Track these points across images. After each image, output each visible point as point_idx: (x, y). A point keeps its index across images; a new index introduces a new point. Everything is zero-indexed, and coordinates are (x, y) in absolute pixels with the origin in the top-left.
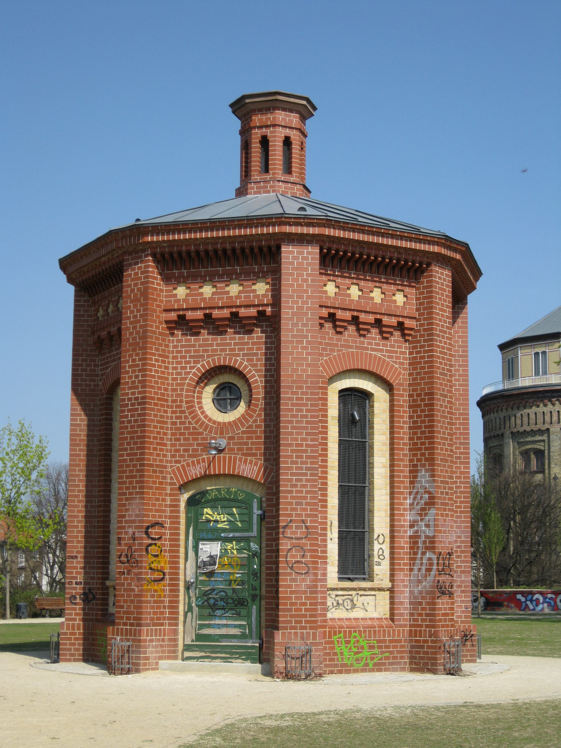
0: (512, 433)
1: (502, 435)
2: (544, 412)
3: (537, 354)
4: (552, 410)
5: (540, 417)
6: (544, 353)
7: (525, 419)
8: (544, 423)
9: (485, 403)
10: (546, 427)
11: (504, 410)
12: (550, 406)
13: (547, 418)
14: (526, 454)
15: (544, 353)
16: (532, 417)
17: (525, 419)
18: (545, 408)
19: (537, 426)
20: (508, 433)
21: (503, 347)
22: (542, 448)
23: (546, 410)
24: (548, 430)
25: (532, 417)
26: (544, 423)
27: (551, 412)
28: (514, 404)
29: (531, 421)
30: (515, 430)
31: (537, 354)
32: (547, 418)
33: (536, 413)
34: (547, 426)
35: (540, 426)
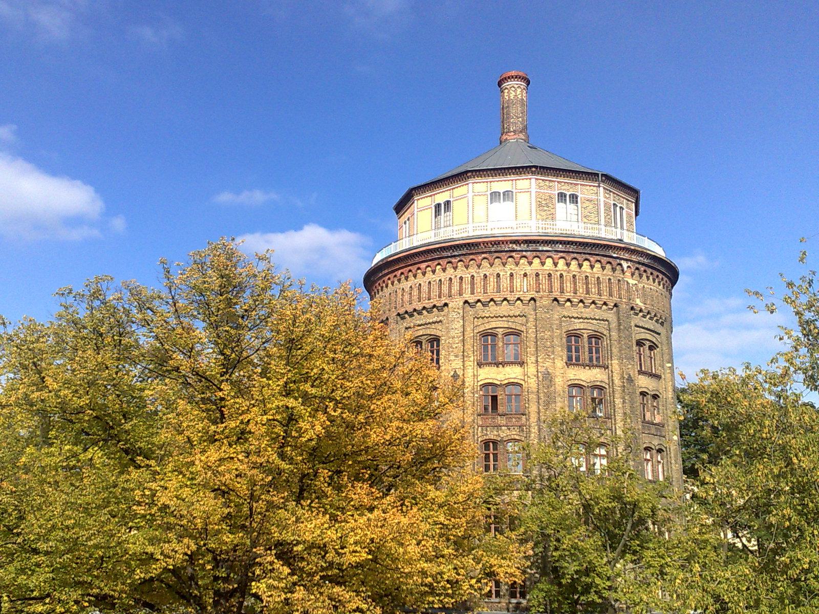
0: (399, 314)
1: (387, 319)
2: (440, 280)
4: (452, 277)
5: (435, 288)
6: (448, 203)
8: (440, 297)
10: (443, 302)
11: (390, 285)
12: (450, 270)
13: (445, 289)
15: (448, 203)
16: (425, 288)
18: (443, 274)
19: (432, 301)
22: (438, 333)
23: (443, 276)
24: (446, 305)
25: (425, 288)
26: (440, 297)
27: (450, 279)
28: (402, 273)
29: (424, 295)
30: (402, 311)
31: (438, 206)
32: (445, 289)
33: (430, 283)
34: (444, 300)
35: (435, 301)
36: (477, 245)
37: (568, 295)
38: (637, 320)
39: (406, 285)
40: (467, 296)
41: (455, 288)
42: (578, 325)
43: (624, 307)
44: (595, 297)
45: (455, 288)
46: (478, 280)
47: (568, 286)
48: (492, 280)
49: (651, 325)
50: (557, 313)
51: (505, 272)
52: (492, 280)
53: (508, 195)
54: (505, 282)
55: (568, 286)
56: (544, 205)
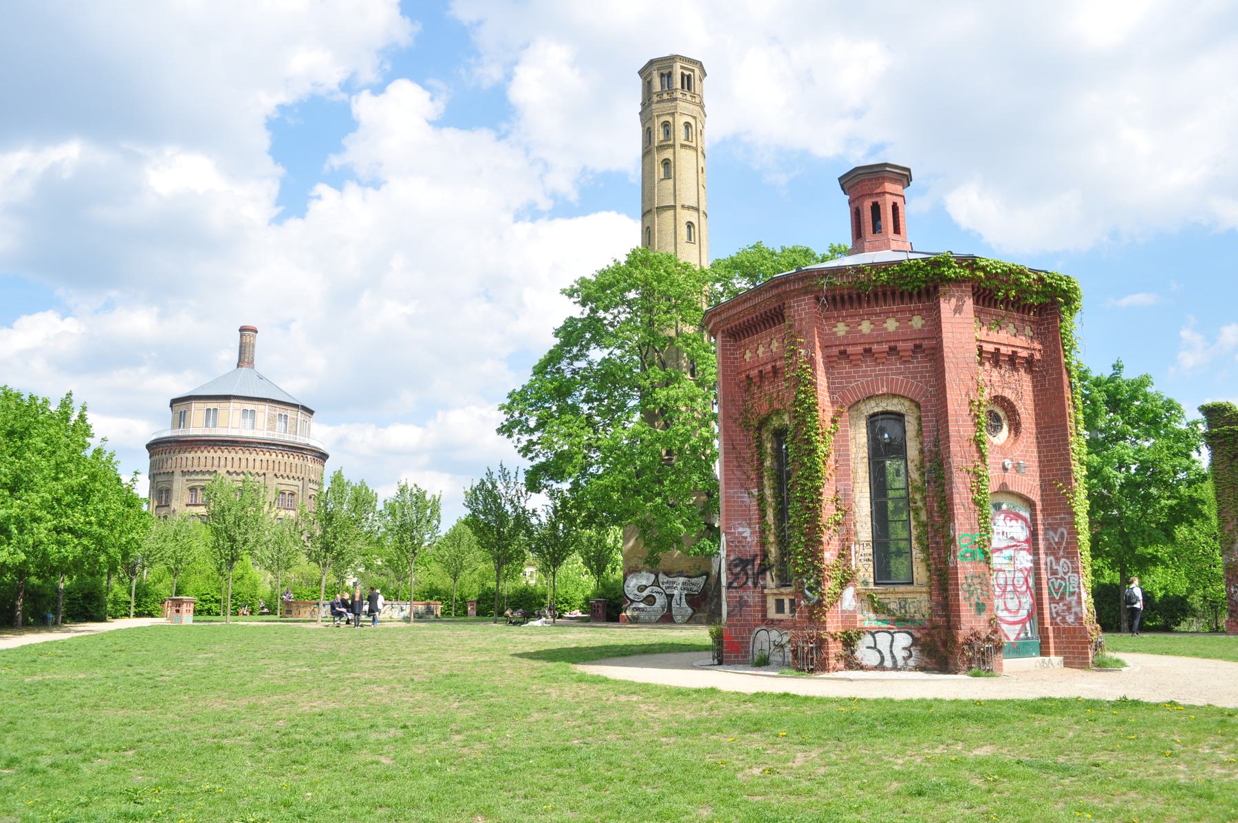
3: (208, 410)
6: (215, 410)
7: (196, 461)
9: (155, 447)
13: (216, 462)
14: (192, 489)
16: (203, 460)
17: (196, 461)
20: (178, 472)
21: (174, 402)
23: (215, 455)
25: (203, 460)
32: (216, 462)
35: (209, 468)
36: (237, 442)
37: (282, 472)
38: (311, 485)
39: (190, 456)
40: (229, 468)
41: (222, 462)
42: (283, 488)
43: (306, 479)
44: (293, 474)
45: (222, 462)
46: (236, 460)
47: (282, 468)
48: (244, 462)
49: (316, 487)
50: (276, 481)
51: (251, 458)
52: (244, 462)
53: (253, 411)
54: (251, 463)
55: (282, 468)
56: (271, 420)
